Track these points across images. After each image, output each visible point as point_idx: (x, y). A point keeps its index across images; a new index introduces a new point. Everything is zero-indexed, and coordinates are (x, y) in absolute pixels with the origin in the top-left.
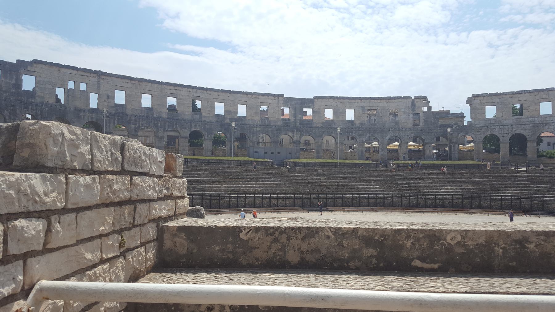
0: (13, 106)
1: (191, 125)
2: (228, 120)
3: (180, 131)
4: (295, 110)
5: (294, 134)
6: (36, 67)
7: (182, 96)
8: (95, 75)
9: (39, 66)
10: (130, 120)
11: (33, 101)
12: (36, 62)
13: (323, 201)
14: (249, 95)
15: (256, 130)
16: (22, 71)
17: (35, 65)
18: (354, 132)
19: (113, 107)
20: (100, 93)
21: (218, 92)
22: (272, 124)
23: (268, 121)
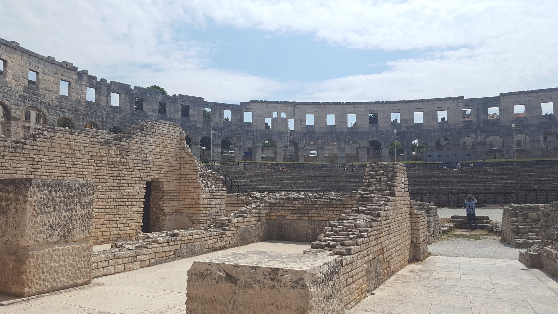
0: (239, 134)
1: (368, 136)
2: (404, 128)
3: (358, 142)
4: (478, 110)
5: (477, 135)
6: (252, 106)
7: (360, 112)
8: (291, 105)
9: (254, 104)
10: (318, 137)
11: (251, 129)
12: (252, 102)
13: (481, 198)
14: (425, 103)
15: (434, 134)
16: (244, 109)
17: (251, 104)
18: (553, 127)
19: (305, 128)
20: (296, 118)
21: (393, 104)
22: (451, 128)
23: (446, 125)
